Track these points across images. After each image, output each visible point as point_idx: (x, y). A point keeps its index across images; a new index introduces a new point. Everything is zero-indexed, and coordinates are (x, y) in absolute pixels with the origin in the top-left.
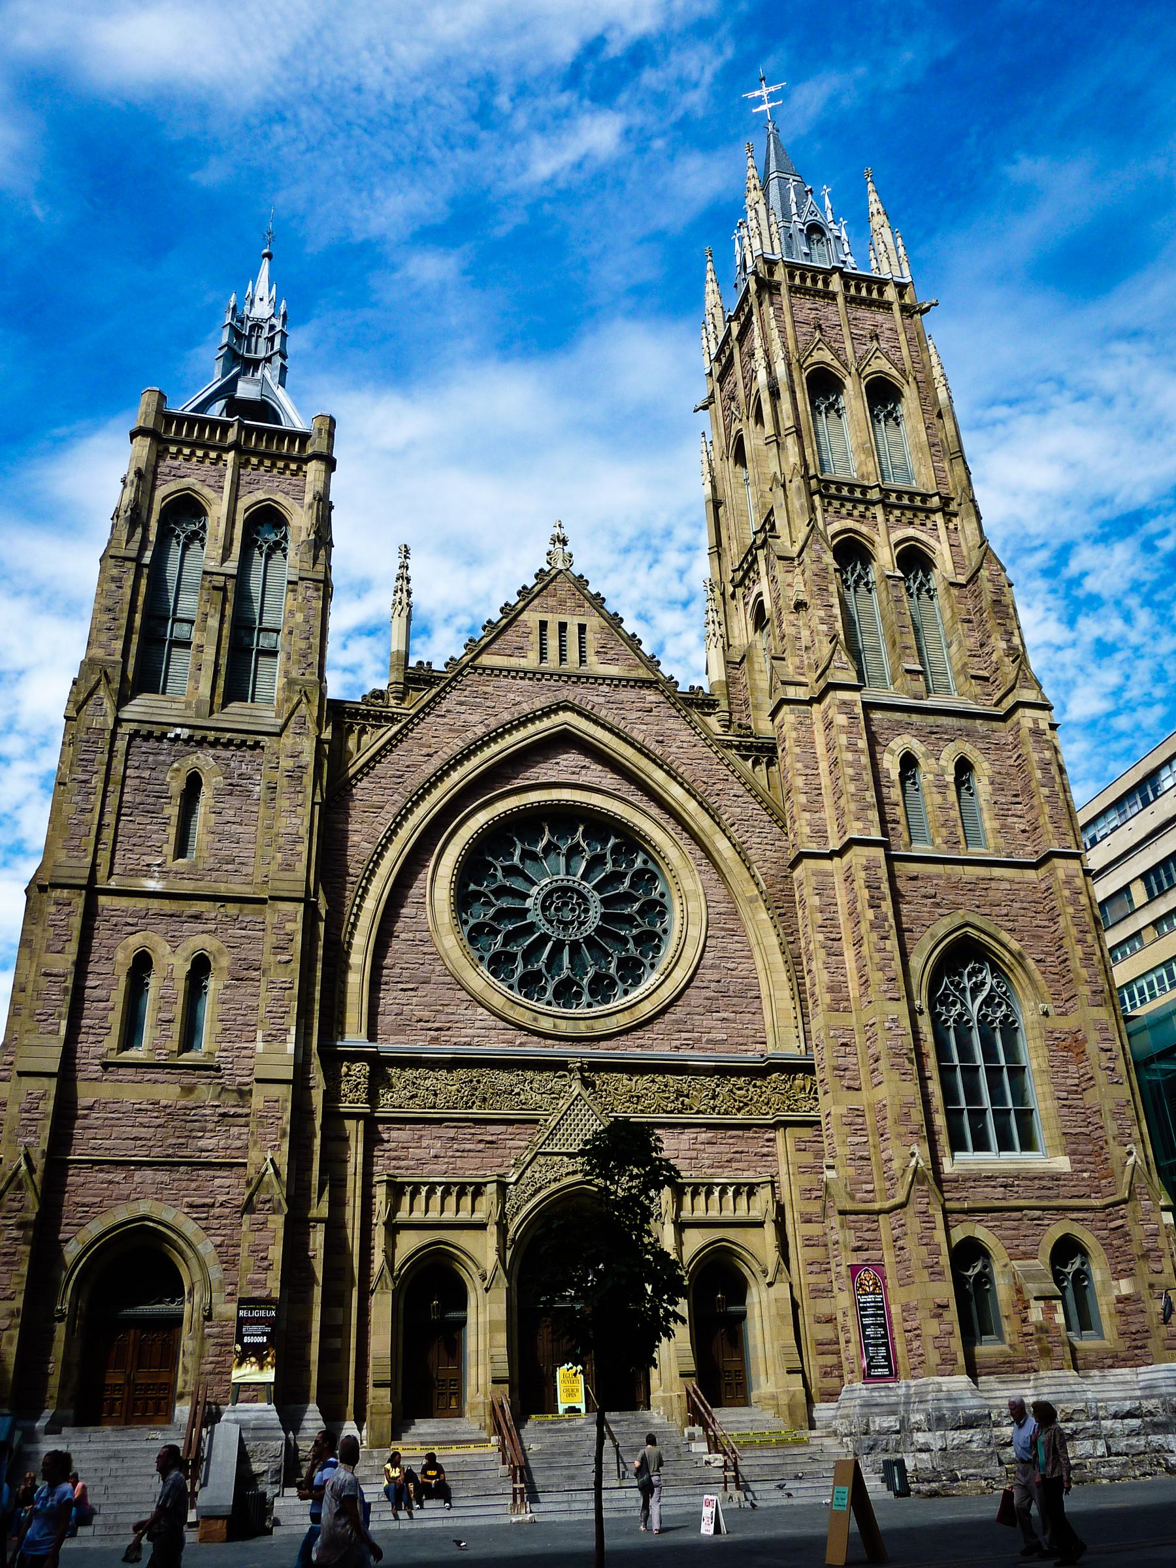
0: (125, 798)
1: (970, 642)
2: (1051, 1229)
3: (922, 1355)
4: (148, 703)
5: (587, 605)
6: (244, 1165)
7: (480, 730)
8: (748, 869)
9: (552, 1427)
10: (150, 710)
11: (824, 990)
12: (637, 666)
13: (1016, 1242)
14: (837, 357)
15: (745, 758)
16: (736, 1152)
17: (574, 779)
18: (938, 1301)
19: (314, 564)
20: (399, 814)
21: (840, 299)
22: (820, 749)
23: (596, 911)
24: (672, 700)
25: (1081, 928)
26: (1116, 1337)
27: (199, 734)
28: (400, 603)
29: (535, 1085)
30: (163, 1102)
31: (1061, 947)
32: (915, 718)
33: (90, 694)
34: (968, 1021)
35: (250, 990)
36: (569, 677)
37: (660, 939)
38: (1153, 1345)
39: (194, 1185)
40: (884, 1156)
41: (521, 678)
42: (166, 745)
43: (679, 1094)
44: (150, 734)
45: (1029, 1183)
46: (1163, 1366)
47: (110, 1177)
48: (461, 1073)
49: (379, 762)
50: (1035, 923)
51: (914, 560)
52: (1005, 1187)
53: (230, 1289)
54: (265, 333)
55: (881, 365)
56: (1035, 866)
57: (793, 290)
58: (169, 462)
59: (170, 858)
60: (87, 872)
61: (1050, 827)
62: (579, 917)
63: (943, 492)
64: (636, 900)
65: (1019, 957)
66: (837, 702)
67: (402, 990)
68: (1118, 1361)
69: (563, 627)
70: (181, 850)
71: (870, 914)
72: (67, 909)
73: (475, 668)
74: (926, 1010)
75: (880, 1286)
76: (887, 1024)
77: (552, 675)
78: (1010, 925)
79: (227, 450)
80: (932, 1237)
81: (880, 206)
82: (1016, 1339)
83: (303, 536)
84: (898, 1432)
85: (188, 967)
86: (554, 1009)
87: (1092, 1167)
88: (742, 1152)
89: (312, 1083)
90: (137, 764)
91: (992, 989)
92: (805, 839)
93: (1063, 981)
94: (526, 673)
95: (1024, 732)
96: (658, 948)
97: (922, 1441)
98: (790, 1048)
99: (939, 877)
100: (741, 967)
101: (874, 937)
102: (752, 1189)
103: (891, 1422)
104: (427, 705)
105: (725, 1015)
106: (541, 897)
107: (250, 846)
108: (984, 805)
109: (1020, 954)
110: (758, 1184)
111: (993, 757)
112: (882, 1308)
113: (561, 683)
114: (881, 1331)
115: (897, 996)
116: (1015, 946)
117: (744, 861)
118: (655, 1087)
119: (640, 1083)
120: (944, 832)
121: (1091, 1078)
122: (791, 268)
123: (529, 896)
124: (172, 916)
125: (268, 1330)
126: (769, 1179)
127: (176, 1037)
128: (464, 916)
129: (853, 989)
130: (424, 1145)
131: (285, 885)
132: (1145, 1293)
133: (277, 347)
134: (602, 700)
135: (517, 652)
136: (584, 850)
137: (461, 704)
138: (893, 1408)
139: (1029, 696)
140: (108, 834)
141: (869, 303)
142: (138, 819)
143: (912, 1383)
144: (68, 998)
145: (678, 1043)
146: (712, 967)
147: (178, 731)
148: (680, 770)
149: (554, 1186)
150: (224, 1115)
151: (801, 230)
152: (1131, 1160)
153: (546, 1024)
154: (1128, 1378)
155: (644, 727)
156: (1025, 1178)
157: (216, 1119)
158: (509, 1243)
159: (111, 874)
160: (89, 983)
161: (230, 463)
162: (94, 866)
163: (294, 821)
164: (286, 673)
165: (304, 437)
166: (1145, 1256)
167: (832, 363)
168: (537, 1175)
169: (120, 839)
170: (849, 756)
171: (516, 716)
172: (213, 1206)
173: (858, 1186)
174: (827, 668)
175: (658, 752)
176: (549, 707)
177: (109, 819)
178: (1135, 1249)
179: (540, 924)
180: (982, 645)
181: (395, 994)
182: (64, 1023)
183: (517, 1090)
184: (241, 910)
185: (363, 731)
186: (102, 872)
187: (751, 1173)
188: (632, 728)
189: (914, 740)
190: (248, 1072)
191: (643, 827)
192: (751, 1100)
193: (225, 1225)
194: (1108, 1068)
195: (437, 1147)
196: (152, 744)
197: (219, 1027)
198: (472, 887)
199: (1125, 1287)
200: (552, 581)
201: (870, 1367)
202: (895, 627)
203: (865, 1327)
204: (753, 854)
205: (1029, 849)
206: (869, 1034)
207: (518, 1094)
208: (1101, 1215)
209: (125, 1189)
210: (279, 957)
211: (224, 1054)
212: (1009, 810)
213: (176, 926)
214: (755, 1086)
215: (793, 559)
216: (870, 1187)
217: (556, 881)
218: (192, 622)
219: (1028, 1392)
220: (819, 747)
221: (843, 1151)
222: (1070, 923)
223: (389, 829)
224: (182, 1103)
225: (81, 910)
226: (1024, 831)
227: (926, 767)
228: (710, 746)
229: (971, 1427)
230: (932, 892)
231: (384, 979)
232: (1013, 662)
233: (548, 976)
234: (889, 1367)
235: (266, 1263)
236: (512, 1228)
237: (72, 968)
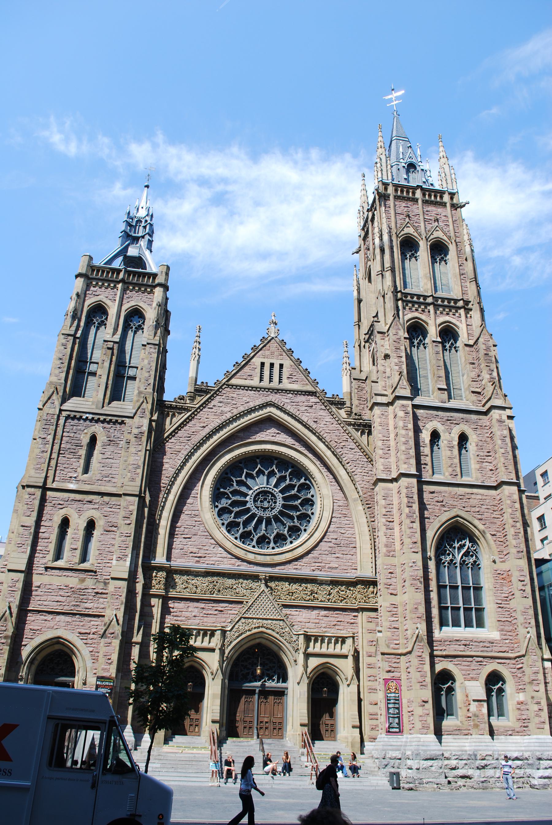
0: (62, 446)
1: (473, 374)
2: (486, 666)
3: (413, 724)
4: (75, 402)
5: (284, 354)
6: (103, 616)
7: (229, 415)
8: (354, 485)
9: (239, 744)
10: (75, 405)
11: (383, 546)
12: (307, 384)
13: (469, 672)
14: (416, 230)
15: (357, 430)
16: (338, 621)
17: (273, 439)
19: (155, 336)
20: (187, 455)
21: (420, 202)
22: (391, 427)
23: (280, 502)
24: (323, 401)
25: (514, 520)
26: (515, 720)
27: (96, 417)
28: (195, 354)
29: (243, 585)
30: (71, 586)
31: (504, 528)
32: (440, 413)
33: (49, 398)
34: (455, 563)
35: (113, 536)
36: (273, 390)
37: (310, 518)
38: (532, 726)
39: (82, 624)
40: (405, 628)
41: (250, 390)
42: (82, 422)
43: (312, 592)
44: (75, 417)
45: (477, 644)
46: (535, 736)
47: (45, 618)
48: (210, 579)
49: (180, 430)
50: (493, 516)
51: (448, 334)
52: (465, 645)
53: (95, 671)
54: (143, 224)
55: (438, 234)
56: (495, 488)
57: (396, 198)
58: (92, 288)
59: (80, 474)
60: (43, 480)
61: (503, 469)
62: (271, 505)
63: (465, 298)
64: (300, 498)
65: (483, 533)
66: (400, 405)
67: (184, 538)
68: (513, 732)
69: (272, 365)
70: (86, 470)
71: (407, 510)
72: (33, 497)
73: (228, 385)
74: (433, 558)
75: (398, 689)
76: (411, 564)
77: (265, 389)
78: (480, 517)
79: (119, 282)
80: (423, 668)
81: (444, 153)
82: (464, 719)
83: (151, 323)
84: (400, 759)
85: (85, 525)
86: (257, 550)
87: (511, 638)
88: (341, 621)
89: (138, 580)
90: (68, 430)
91: (468, 548)
92: (380, 472)
93: (505, 545)
94: (252, 388)
95: (494, 421)
96: (309, 521)
97: (409, 764)
98: (367, 573)
99: (446, 492)
100: (348, 532)
101: (408, 521)
102: (343, 640)
103: (397, 754)
104: (204, 403)
105: (337, 555)
106: (253, 496)
107: (117, 469)
108: (472, 456)
109: (484, 531)
110: (347, 637)
111: (478, 433)
112: (398, 700)
113: (269, 393)
114: (397, 711)
115: (416, 550)
116: (481, 527)
117: (352, 481)
118: (301, 589)
119: (295, 587)
120: (450, 469)
121: (513, 594)
122: (396, 186)
123: (248, 495)
124: (79, 501)
125: (109, 691)
126: (352, 635)
127: (78, 556)
128: (217, 504)
129: (398, 546)
130: (190, 610)
131: (130, 488)
132: (530, 700)
133: (147, 231)
134: (288, 401)
135: (249, 378)
136: (276, 474)
137: (221, 402)
138: (399, 748)
139: (499, 402)
140: (53, 463)
141: (435, 203)
142: (68, 456)
143: (410, 736)
144: (31, 537)
145: (313, 568)
146: (334, 532)
147: (87, 415)
148: (324, 436)
149: (248, 633)
150: (97, 593)
151: (404, 167)
152: (528, 636)
153: (251, 557)
154: (519, 741)
155: (308, 414)
157: (94, 594)
158: (225, 658)
159: (54, 481)
160: (41, 531)
161: (120, 289)
162: (46, 477)
163: (137, 458)
164: (139, 388)
165: (155, 276)
166: (531, 682)
167: (413, 234)
168: (240, 628)
169: (59, 465)
170: (403, 432)
171: (247, 408)
172: (89, 634)
173: (392, 641)
174: (396, 388)
175: (314, 427)
176: (263, 404)
177: (55, 456)
178: (526, 679)
179: (252, 508)
180: (479, 376)
181: (181, 540)
182: (29, 548)
183: (235, 587)
184: (110, 499)
185: (174, 416)
186: (50, 480)
187: (344, 632)
188: (302, 415)
189: (439, 424)
190: (109, 574)
191: (304, 463)
192: (348, 596)
193: (95, 643)
194: (521, 590)
195: (196, 612)
196: (76, 421)
197: (98, 552)
198: (222, 490)
199: (521, 697)
200: (268, 342)
201: (389, 727)
202: (435, 367)
203: (389, 708)
204: (357, 478)
205: (493, 479)
206: (403, 568)
207: (236, 589)
208: (513, 662)
209: (51, 624)
210: (126, 522)
211: (99, 565)
212: (484, 459)
213: (81, 506)
214: (350, 590)
215: (385, 333)
216: (397, 642)
217: (262, 488)
218: (98, 363)
219: (467, 744)
220: (392, 426)
221: (386, 624)
222: (509, 517)
223: (182, 462)
224: (79, 587)
225: (39, 497)
226: (491, 470)
227: (444, 436)
228: (340, 424)
229: (433, 759)
230: (441, 499)
231: (176, 533)
232: (492, 385)
233: (254, 534)
234: (399, 728)
235: (110, 661)
236: (227, 652)
237: (34, 524)
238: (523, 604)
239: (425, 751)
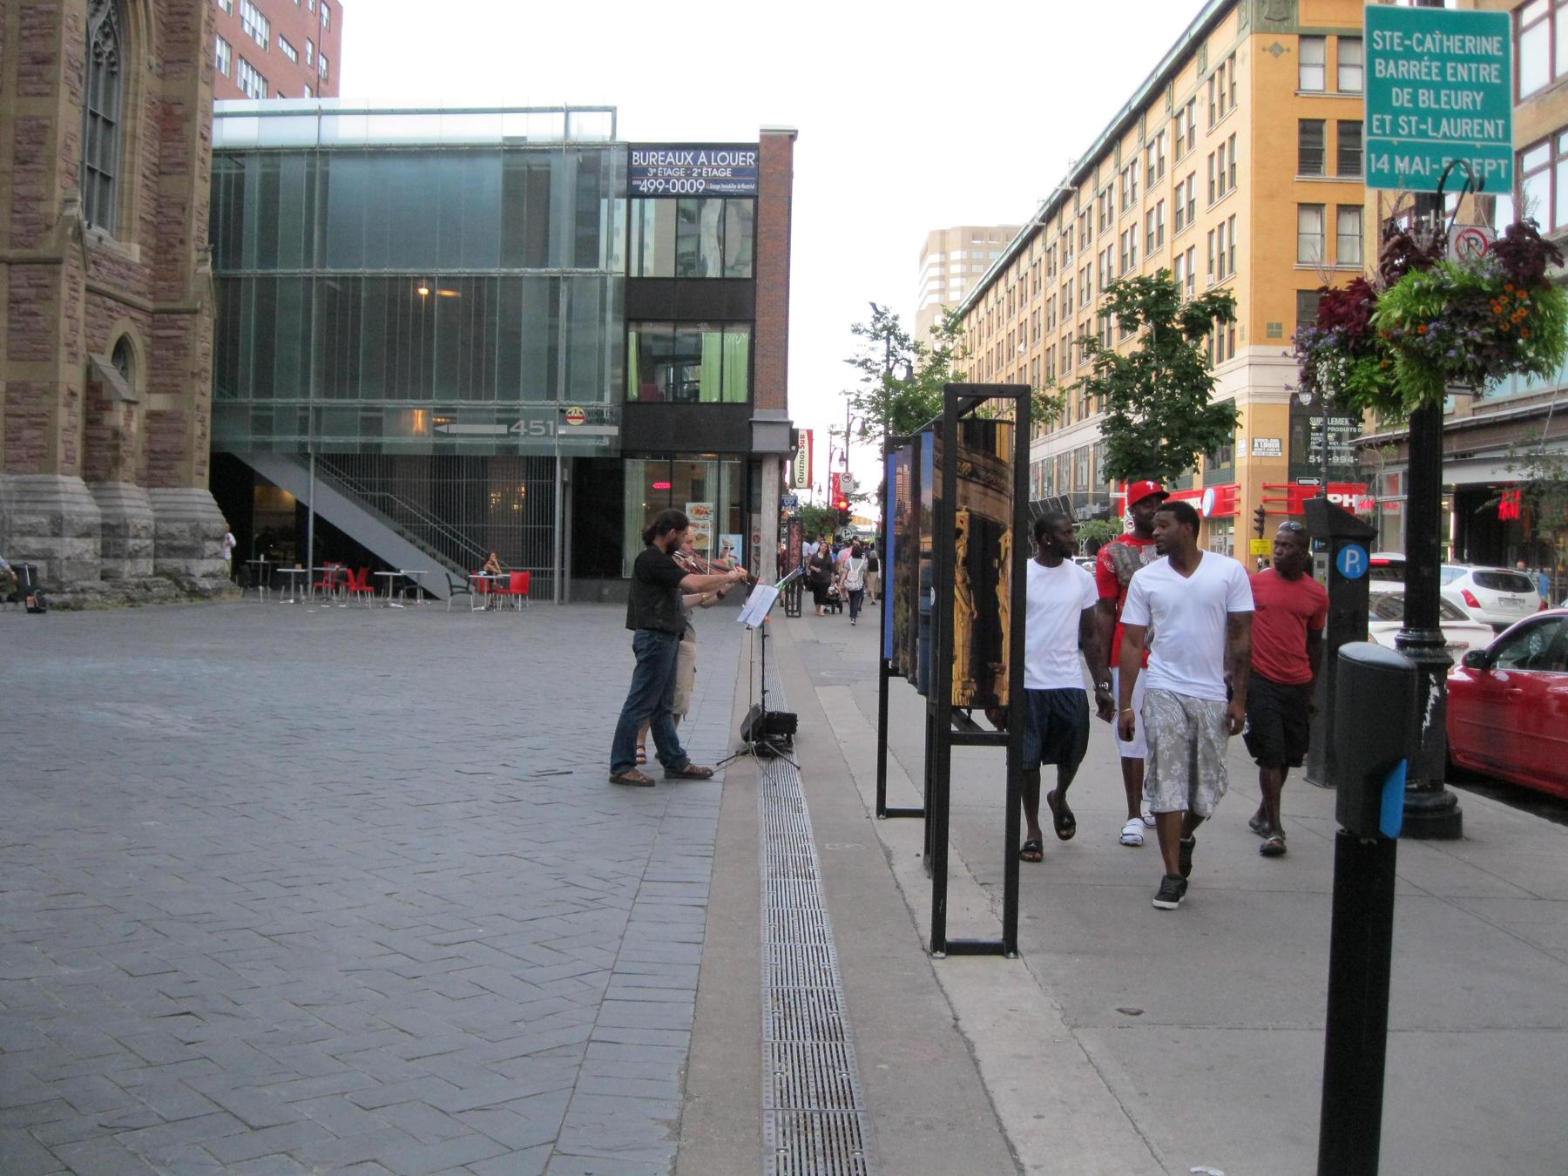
3: (41, 447)
18: (73, 387)
40: (22, 190)
80: (74, 310)
91: (109, 16)
143: (8, 477)
156: (110, 260)
199: (159, 402)
206: (36, 21)
238: (201, 192)
239: (80, 515)
